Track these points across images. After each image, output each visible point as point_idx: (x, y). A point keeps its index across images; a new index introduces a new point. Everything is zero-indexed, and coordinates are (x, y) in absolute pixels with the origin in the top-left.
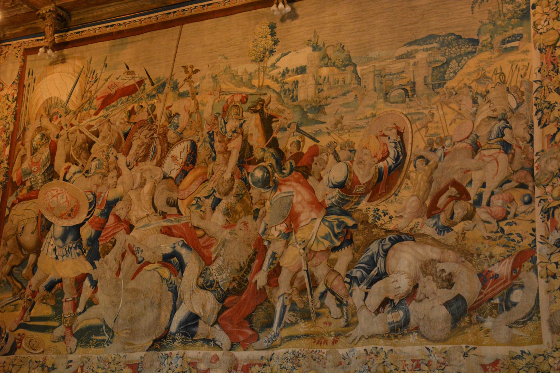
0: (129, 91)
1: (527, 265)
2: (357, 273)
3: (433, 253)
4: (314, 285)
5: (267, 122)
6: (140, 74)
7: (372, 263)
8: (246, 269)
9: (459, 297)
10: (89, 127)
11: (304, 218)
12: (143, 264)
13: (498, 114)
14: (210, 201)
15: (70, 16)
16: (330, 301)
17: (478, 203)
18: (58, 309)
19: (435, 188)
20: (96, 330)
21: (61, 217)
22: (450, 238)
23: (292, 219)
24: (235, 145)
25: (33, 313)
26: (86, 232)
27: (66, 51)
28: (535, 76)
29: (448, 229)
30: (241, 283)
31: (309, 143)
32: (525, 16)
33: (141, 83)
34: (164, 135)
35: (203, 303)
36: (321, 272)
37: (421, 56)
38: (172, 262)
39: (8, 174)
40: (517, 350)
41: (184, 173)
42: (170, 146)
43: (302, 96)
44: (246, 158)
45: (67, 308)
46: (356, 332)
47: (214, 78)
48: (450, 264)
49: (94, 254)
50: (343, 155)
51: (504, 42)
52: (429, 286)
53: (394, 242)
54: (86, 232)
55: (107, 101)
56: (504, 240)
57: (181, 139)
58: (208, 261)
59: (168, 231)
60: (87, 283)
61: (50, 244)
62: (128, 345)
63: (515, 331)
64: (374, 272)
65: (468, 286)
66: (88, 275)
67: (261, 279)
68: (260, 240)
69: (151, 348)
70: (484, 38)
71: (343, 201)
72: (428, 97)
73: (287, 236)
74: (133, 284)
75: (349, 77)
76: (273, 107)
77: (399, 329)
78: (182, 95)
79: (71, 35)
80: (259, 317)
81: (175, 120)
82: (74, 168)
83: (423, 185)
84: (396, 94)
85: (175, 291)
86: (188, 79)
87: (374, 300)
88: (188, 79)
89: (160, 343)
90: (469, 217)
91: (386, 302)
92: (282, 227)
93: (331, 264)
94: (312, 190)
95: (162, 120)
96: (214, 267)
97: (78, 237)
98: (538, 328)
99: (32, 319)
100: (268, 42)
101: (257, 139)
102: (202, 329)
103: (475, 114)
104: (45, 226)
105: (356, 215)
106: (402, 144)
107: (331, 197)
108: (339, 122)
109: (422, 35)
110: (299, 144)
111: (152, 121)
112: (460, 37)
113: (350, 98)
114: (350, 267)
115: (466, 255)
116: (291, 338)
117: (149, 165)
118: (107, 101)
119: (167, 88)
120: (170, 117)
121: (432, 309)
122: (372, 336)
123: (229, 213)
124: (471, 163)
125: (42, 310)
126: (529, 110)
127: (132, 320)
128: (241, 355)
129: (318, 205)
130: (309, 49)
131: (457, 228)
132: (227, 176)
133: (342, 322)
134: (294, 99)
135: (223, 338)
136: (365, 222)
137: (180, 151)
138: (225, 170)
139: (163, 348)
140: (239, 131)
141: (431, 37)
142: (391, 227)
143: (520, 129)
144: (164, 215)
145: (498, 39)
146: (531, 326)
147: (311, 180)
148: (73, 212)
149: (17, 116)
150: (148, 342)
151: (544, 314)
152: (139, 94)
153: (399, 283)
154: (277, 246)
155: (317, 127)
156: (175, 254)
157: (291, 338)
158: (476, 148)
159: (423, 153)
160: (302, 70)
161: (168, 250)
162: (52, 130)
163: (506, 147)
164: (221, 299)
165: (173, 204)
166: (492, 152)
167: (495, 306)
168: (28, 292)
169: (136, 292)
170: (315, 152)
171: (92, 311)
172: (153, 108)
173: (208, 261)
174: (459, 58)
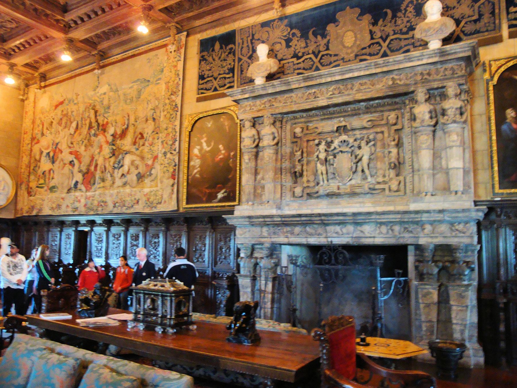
0: (62, 103)
1: (156, 161)
2: (116, 166)
3: (134, 158)
4: (105, 171)
5: (96, 112)
6: (65, 97)
7: (119, 162)
8: (90, 165)
9: (139, 173)
10: (52, 117)
11: (103, 147)
12: (65, 164)
13: (152, 108)
14: (81, 142)
15: (46, 75)
16: (109, 175)
17: (146, 140)
18: (45, 180)
19: (136, 136)
20: (54, 187)
21: (45, 149)
22: (138, 152)
23: (101, 147)
24: (88, 122)
25: (40, 182)
26: (51, 154)
27: (46, 89)
28: (163, 93)
29: (137, 149)
30: (88, 170)
31: (106, 120)
32: (162, 71)
33: (65, 100)
34: (70, 119)
35: (79, 177)
36: (107, 165)
37: (135, 87)
38: (71, 163)
39: (32, 135)
40: (152, 189)
41: (75, 132)
42: (71, 123)
43: (104, 103)
44: (90, 127)
45: (47, 179)
46: (116, 185)
47: (83, 97)
48: (138, 162)
49: (53, 162)
50: (114, 124)
51: (156, 81)
52: (133, 169)
53: (126, 154)
54: (51, 154)
55: (57, 106)
56: (151, 153)
57: (74, 120)
58: (80, 163)
59: (71, 153)
60: (52, 172)
61: (43, 159)
62: (62, 192)
63: (152, 183)
64: (120, 165)
65: (142, 169)
66: (51, 169)
67: (92, 168)
68: (93, 155)
69: (67, 193)
70: (151, 80)
71: (113, 141)
72: (136, 102)
73: (99, 153)
74: (62, 172)
75: (117, 95)
76: (97, 108)
77: (125, 184)
78: (75, 104)
79: (48, 82)
80: (92, 181)
81: (73, 113)
82: (48, 132)
83: (132, 134)
84: (128, 101)
85: (72, 173)
86: (77, 99)
87: (120, 175)
88: (77, 99)
89: (69, 191)
90: (143, 145)
91: (123, 175)
92: (98, 150)
93: (109, 162)
94: (106, 137)
95: (70, 114)
96: (82, 165)
97: (49, 156)
98: (157, 183)
99: (40, 184)
100: (97, 84)
101: (93, 120)
102: (80, 186)
103: (147, 108)
104: (41, 153)
105: (116, 145)
106: (128, 119)
107: (110, 139)
108: (113, 112)
109: (136, 79)
110: (103, 121)
111: (67, 114)
112: (145, 80)
113: (117, 103)
114: (114, 163)
115: (142, 158)
116: (99, 188)
117: (66, 130)
118: (57, 106)
119: (71, 102)
120: (72, 112)
121: (132, 177)
122: (119, 187)
123: (86, 146)
124: (145, 126)
125: (42, 181)
126: (161, 106)
127: (62, 184)
128: (89, 194)
129: (107, 142)
130: (107, 85)
131: (140, 149)
132: (86, 133)
133: (111, 182)
134: (103, 104)
135: (84, 188)
136: (118, 148)
137: (74, 125)
138: (85, 131)
139: (70, 192)
140: (88, 117)
141: (138, 80)
142: (125, 149)
143: (158, 114)
144: (70, 147)
145: (155, 80)
146: (156, 181)
147: (106, 134)
148: (48, 148)
149: (34, 113)
150: (66, 191)
151: (159, 177)
152: (64, 104)
153: (126, 168)
154: (96, 158)
155: (109, 114)
156: (73, 161)
157: (99, 188)
158: (147, 120)
159: (133, 123)
160: (105, 94)
161: (71, 160)
162: (43, 119)
163: (154, 119)
164: (83, 176)
165: (72, 143)
166: (150, 122)
167: (148, 175)
168: (38, 175)
169: (63, 174)
170: (107, 123)
171: (54, 180)
172: (68, 109)
173: (80, 163)
174: (144, 87)
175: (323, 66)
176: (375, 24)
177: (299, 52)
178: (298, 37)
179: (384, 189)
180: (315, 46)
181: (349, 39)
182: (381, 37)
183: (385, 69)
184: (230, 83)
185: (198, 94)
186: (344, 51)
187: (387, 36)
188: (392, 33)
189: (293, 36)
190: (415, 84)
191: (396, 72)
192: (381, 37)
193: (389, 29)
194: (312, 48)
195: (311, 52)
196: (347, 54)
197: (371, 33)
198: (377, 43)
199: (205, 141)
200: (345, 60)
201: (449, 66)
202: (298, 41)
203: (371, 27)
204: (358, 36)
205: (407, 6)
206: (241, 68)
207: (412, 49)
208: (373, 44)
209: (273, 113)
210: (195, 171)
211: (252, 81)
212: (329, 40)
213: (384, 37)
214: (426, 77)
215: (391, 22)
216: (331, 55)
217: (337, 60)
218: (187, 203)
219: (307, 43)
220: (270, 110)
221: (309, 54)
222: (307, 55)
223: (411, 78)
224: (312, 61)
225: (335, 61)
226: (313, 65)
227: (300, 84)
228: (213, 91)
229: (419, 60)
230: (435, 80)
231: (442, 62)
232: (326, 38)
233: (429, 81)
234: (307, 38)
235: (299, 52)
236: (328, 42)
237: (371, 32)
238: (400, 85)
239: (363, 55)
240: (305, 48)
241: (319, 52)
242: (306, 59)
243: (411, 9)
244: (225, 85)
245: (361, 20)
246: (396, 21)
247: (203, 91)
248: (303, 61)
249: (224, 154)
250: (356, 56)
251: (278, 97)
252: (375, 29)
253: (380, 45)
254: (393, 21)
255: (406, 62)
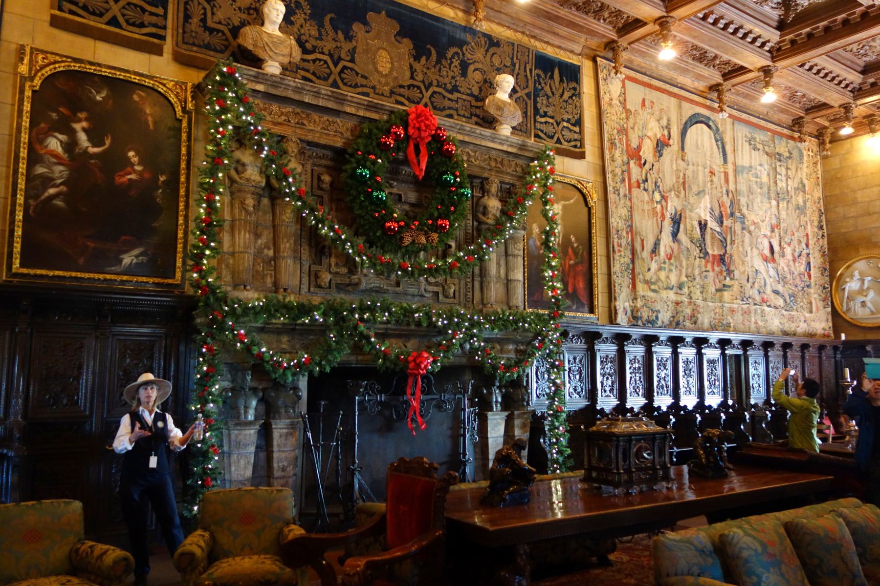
175: (345, 84)
176: (417, 58)
177: (307, 41)
178: (305, 14)
179: (437, 294)
180: (334, 46)
181: (384, 63)
182: (423, 82)
183: (467, 139)
184: (155, 26)
185: (60, 9)
186: (376, 76)
187: (431, 84)
188: (435, 83)
189: (297, 7)
190: (490, 170)
191: (471, 147)
192: (423, 82)
193: (433, 76)
194: (328, 45)
195: (326, 51)
196: (380, 83)
197: (413, 71)
198: (419, 88)
199: (84, 130)
200: (377, 91)
201: (520, 162)
202: (305, 20)
203: (412, 60)
204: (396, 64)
205: (453, 57)
206: (186, 9)
207: (456, 117)
208: (414, 86)
209: (303, 138)
210: (52, 191)
211: (256, 62)
212: (355, 47)
213: (427, 83)
214: (499, 165)
215: (435, 67)
216: (357, 74)
217: (366, 86)
218: (22, 265)
219: (320, 34)
220: (298, 131)
221: (323, 53)
222: (320, 53)
223: (484, 161)
224: (328, 67)
225: (362, 86)
226: (329, 75)
227: (358, 109)
228: (108, 23)
229: (500, 143)
230: (508, 174)
231: (515, 155)
232: (351, 41)
233: (502, 172)
234: (321, 25)
235: (307, 41)
236: (355, 48)
237: (411, 67)
238: (476, 166)
239: (400, 95)
240: (317, 39)
241: (340, 59)
242: (320, 60)
243: (456, 63)
244: (142, 25)
245: (399, 42)
246: (440, 69)
247: (74, 8)
248: (314, 61)
249: (140, 173)
250: (392, 92)
251: (315, 116)
252: (416, 66)
253: (421, 92)
254: (438, 67)
255: (489, 140)
